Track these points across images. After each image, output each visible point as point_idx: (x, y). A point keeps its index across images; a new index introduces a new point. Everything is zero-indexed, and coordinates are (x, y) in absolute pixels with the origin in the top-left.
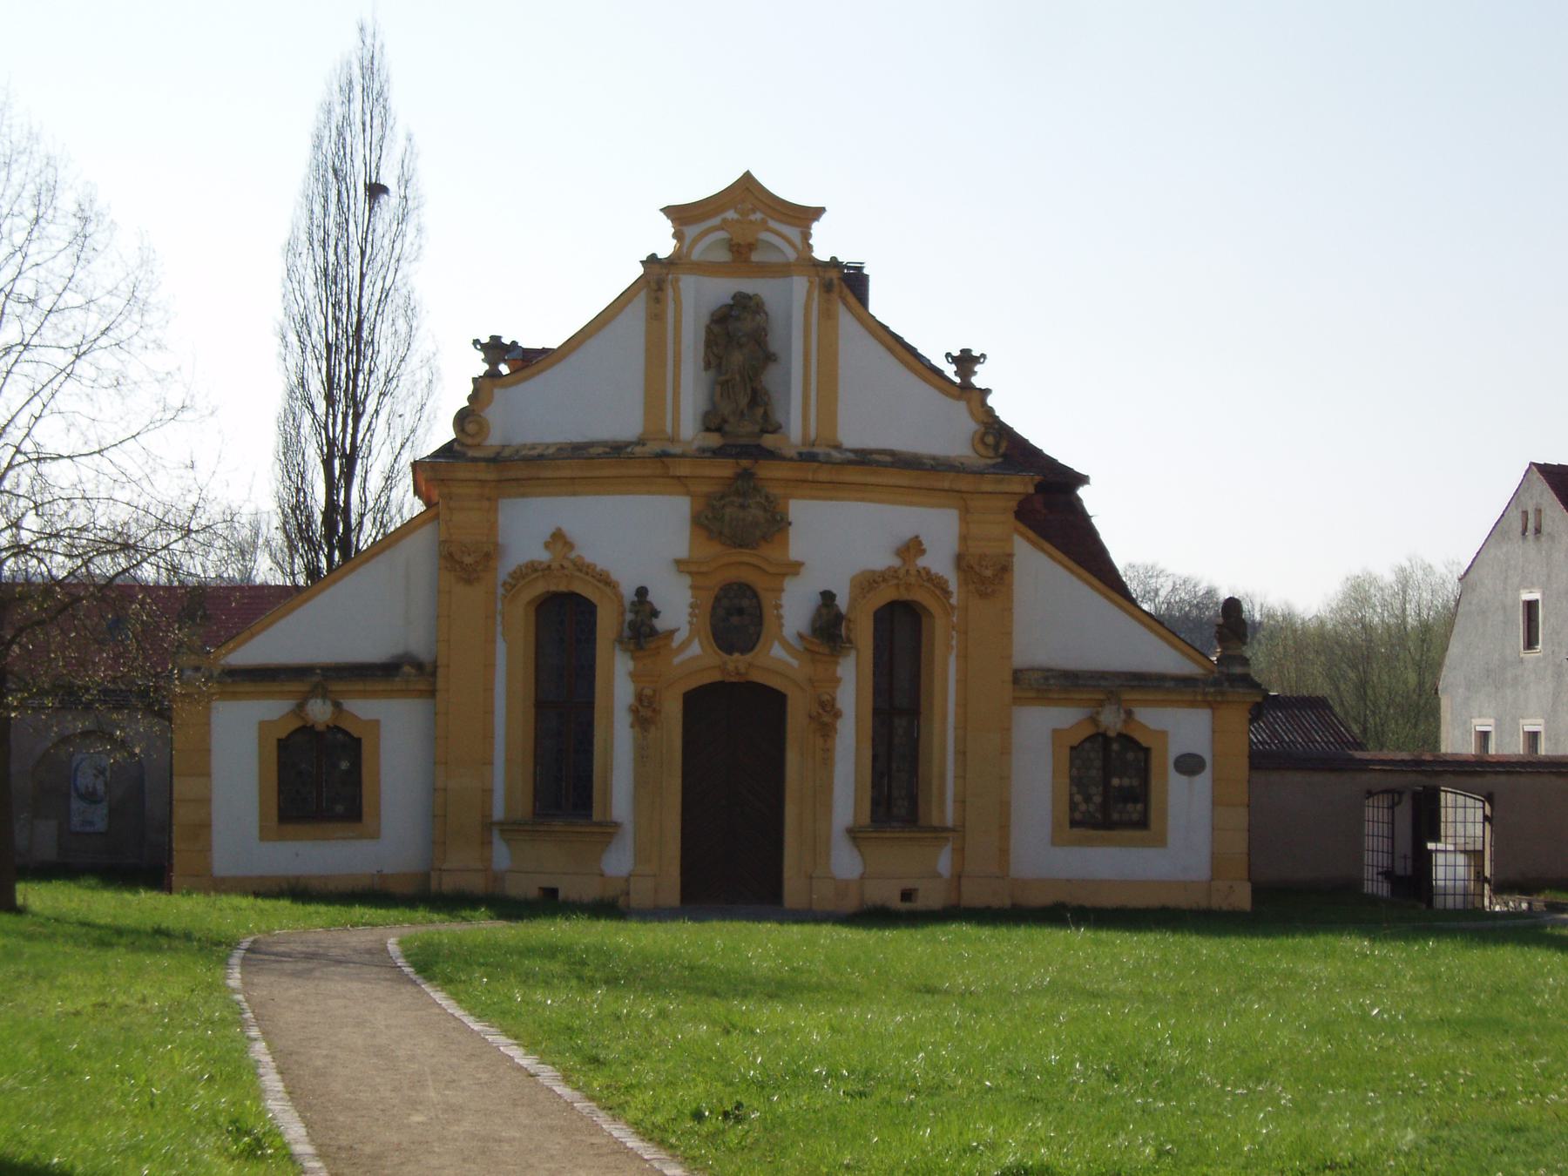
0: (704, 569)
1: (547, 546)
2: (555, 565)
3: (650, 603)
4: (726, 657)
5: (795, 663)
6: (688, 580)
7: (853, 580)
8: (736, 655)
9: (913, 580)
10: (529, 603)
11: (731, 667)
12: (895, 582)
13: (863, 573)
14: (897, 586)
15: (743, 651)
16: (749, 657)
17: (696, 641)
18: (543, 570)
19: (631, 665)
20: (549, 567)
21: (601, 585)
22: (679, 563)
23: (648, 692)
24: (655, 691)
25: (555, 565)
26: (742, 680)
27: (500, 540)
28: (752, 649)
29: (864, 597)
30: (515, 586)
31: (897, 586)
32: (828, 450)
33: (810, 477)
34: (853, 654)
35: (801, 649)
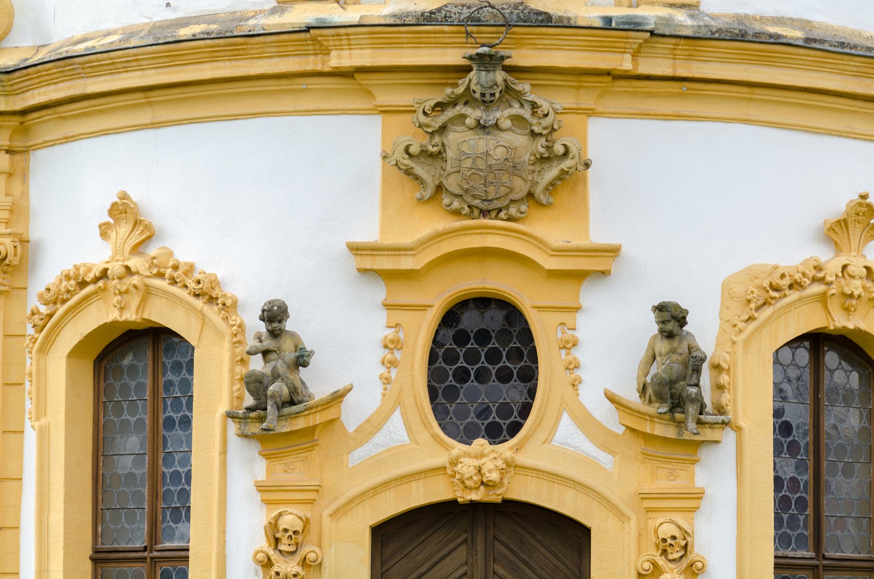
0: (407, 263)
1: (104, 231)
2: (116, 268)
3: (293, 335)
4: (458, 448)
5: (604, 458)
6: (379, 292)
7: (726, 289)
8: (480, 443)
9: (856, 287)
10: (76, 352)
11: (467, 467)
12: (818, 288)
13: (751, 273)
14: (823, 299)
15: (495, 434)
16: (505, 449)
17: (397, 418)
18: (96, 280)
19: (260, 469)
20: (104, 274)
21: (199, 303)
22: (356, 249)
23: (289, 521)
24: (306, 522)
25: (116, 268)
26: (495, 497)
27: (34, 235)
28: (515, 429)
29: (750, 319)
30: (50, 316)
31: (823, 299)
32: (665, 12)
33: (626, 64)
34: (728, 438)
35: (621, 430)
